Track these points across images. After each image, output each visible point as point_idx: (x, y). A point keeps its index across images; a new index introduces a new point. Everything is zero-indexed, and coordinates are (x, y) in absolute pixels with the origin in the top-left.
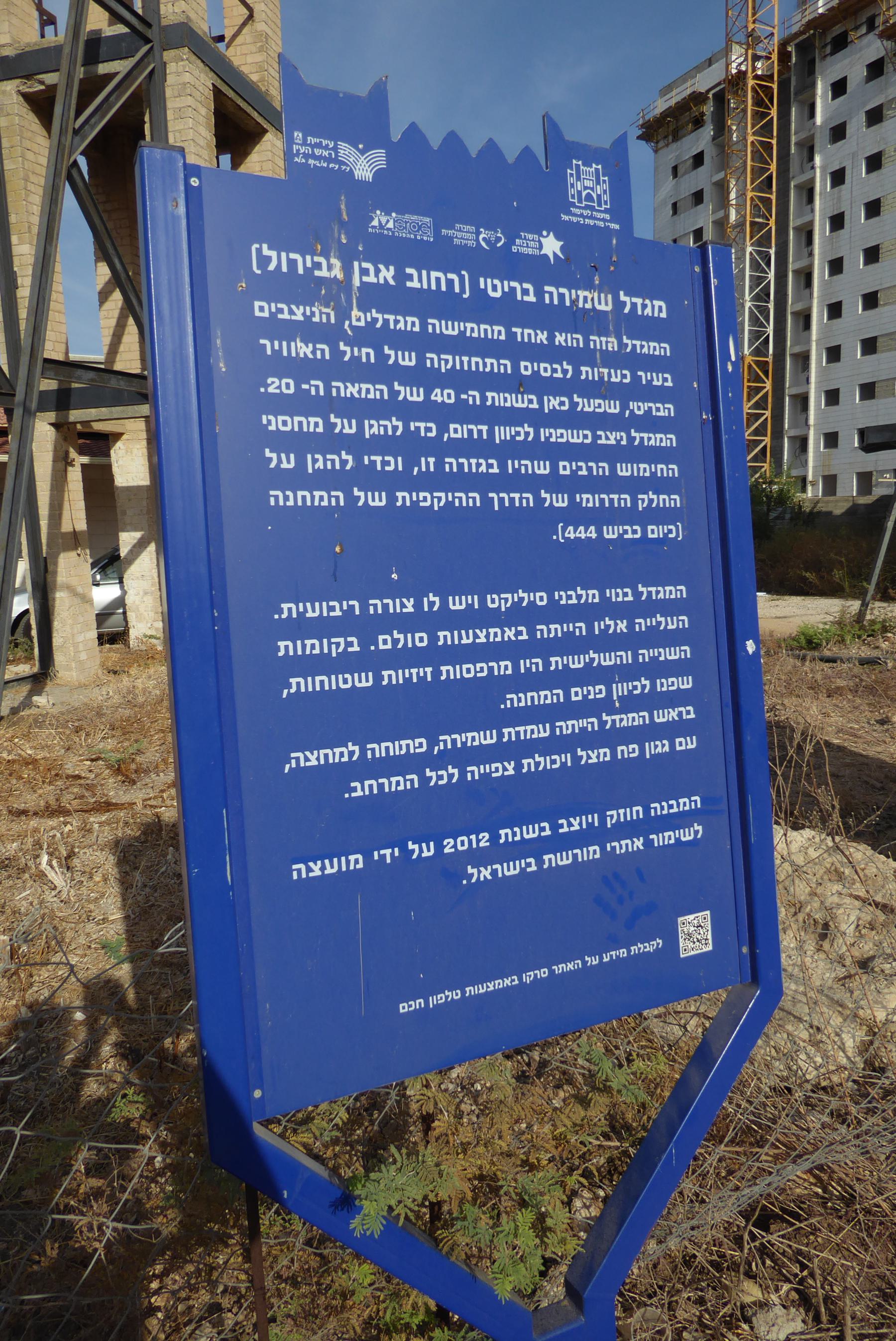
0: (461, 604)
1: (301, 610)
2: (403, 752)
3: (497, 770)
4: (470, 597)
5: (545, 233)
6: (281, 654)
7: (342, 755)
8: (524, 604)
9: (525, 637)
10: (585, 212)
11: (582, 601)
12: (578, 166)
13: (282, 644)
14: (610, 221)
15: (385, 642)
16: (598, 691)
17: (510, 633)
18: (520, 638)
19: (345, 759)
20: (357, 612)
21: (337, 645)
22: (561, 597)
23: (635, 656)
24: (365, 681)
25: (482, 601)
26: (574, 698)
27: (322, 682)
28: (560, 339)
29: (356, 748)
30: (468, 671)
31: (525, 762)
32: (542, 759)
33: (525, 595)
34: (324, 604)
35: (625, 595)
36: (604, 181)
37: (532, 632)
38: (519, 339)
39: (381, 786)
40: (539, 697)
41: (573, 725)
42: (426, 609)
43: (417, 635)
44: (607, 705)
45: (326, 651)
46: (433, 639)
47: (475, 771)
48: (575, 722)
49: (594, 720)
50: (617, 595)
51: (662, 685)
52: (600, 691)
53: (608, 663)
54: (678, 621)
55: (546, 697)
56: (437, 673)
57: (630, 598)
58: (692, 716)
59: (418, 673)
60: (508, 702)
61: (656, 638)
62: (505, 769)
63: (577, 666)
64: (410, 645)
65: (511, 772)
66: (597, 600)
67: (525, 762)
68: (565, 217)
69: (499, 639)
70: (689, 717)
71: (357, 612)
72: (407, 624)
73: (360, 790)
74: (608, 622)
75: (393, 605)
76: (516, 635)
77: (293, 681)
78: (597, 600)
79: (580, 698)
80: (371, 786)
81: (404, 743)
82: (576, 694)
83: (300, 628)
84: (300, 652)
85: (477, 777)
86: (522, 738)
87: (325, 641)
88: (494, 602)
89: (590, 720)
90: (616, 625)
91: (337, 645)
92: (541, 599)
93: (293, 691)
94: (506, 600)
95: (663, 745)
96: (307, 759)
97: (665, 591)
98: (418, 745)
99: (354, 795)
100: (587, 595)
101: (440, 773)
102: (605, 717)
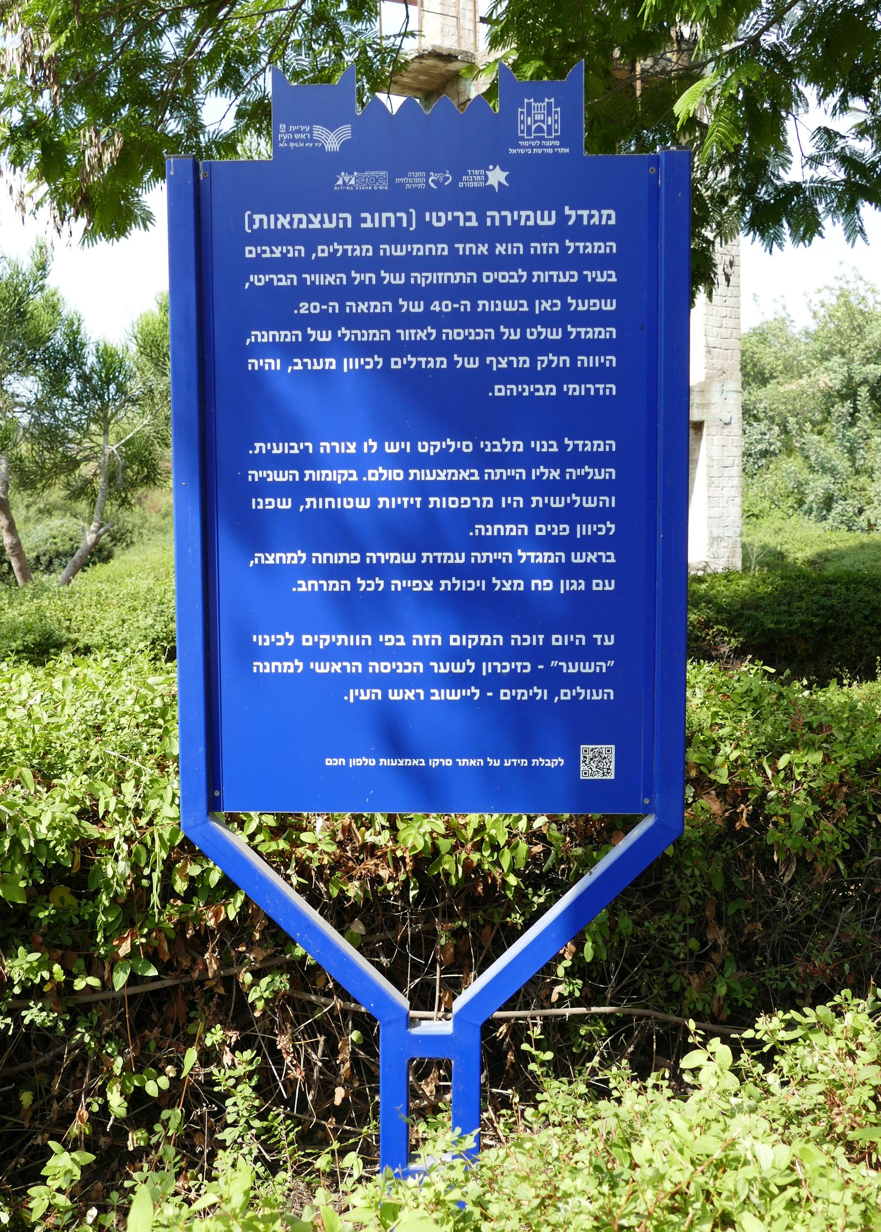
2: (341, 562)
5: (491, 167)
7: (292, 558)
10: (533, 144)
12: (529, 104)
14: (560, 147)
19: (295, 562)
28: (500, 249)
29: (304, 555)
31: (443, 582)
32: (458, 582)
36: (556, 112)
38: (461, 253)
48: (490, 554)
58: (613, 560)
62: (424, 586)
68: (513, 151)
80: (313, 585)
81: (342, 555)
95: (579, 584)
96: (266, 559)
99: (299, 589)
102: (520, 553)
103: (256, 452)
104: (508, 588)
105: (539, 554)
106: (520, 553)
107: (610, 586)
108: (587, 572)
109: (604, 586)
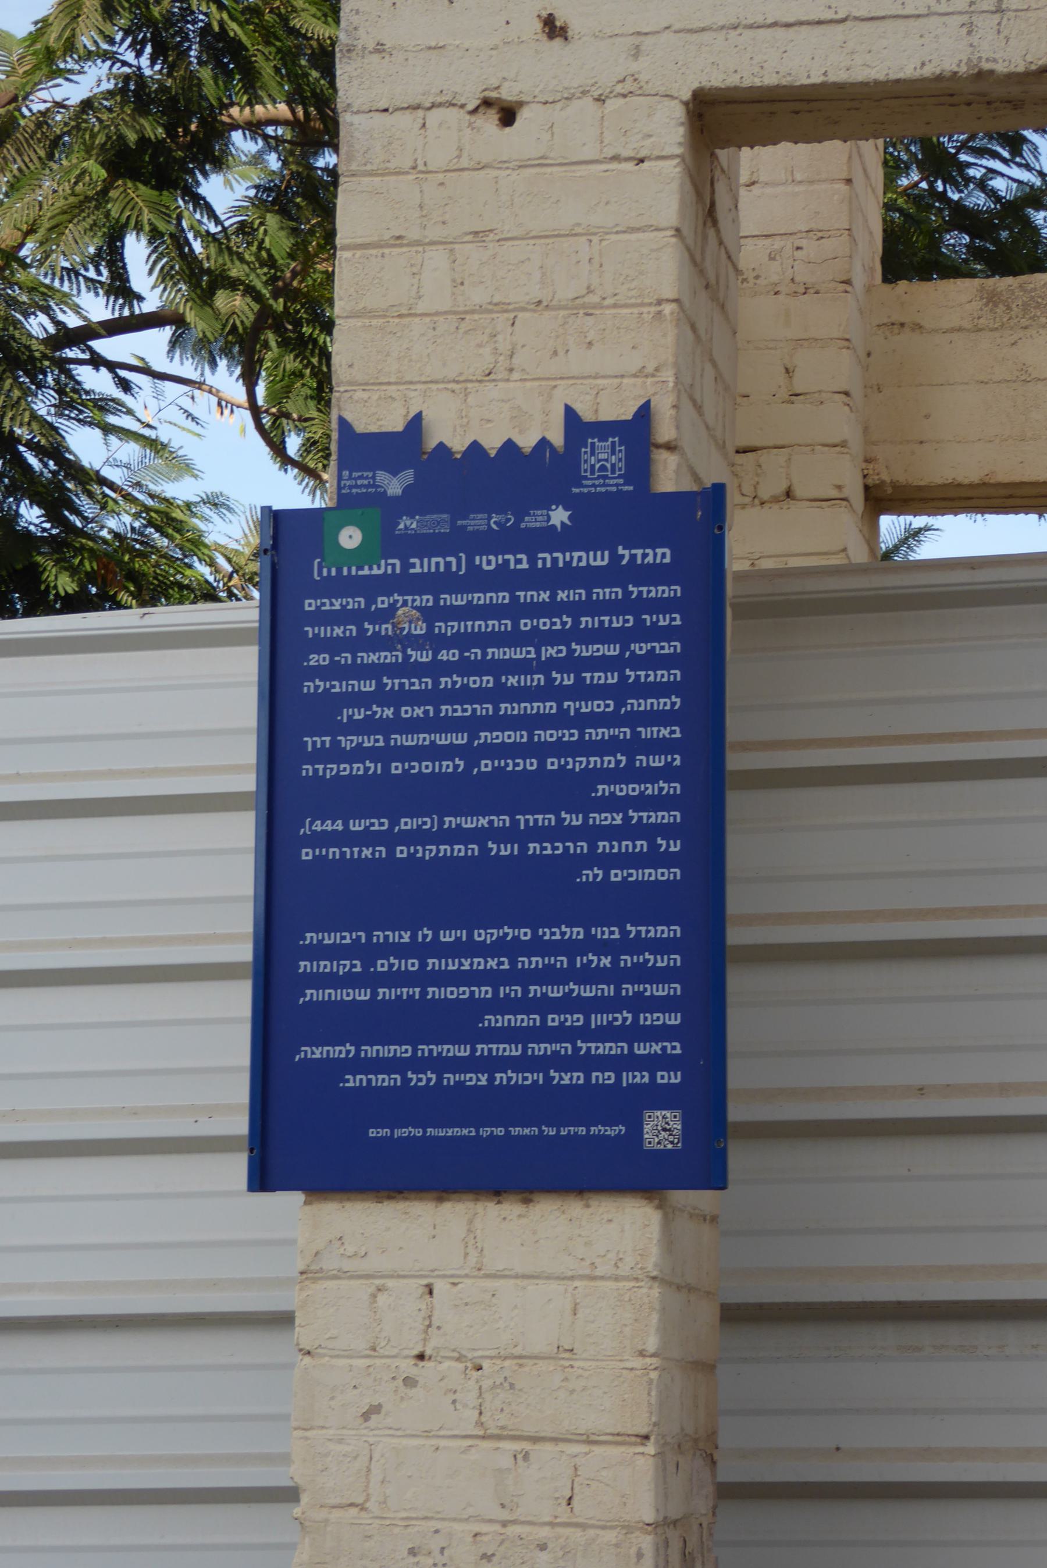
7: (340, 1052)
8: (509, 938)
9: (506, 966)
11: (566, 937)
15: (382, 965)
16: (576, 1020)
17: (492, 963)
18: (502, 967)
19: (343, 1056)
20: (363, 941)
21: (344, 966)
22: (544, 934)
23: (618, 990)
24: (364, 996)
25: (470, 935)
26: (550, 1024)
27: (330, 994)
29: (353, 1048)
31: (498, 1075)
35: (612, 933)
37: (513, 963)
39: (369, 1081)
40: (516, 1020)
42: (420, 940)
43: (410, 961)
44: (586, 1033)
45: (335, 970)
46: (423, 965)
49: (569, 1045)
50: (603, 933)
51: (646, 1019)
53: (588, 994)
54: (669, 959)
55: (522, 1020)
56: (424, 993)
57: (617, 936)
58: (678, 1051)
60: (486, 1022)
61: (643, 974)
62: (478, 1080)
63: (555, 995)
64: (403, 969)
65: (484, 1082)
66: (581, 937)
69: (481, 967)
70: (674, 1052)
71: (363, 941)
72: (402, 951)
73: (352, 1081)
74: (591, 957)
75: (393, 937)
77: (308, 992)
78: (581, 937)
80: (361, 1080)
81: (392, 1048)
84: (315, 970)
87: (335, 963)
88: (480, 936)
89: (563, 1045)
90: (599, 960)
91: (344, 966)
93: (307, 999)
94: (492, 935)
95: (643, 1077)
96: (313, 1053)
98: (404, 1051)
99: (347, 1085)
100: (572, 932)
103: (307, 942)
104: (566, 1082)
106: (579, 1044)
107: (676, 1079)
108: (652, 1063)
109: (669, 1078)
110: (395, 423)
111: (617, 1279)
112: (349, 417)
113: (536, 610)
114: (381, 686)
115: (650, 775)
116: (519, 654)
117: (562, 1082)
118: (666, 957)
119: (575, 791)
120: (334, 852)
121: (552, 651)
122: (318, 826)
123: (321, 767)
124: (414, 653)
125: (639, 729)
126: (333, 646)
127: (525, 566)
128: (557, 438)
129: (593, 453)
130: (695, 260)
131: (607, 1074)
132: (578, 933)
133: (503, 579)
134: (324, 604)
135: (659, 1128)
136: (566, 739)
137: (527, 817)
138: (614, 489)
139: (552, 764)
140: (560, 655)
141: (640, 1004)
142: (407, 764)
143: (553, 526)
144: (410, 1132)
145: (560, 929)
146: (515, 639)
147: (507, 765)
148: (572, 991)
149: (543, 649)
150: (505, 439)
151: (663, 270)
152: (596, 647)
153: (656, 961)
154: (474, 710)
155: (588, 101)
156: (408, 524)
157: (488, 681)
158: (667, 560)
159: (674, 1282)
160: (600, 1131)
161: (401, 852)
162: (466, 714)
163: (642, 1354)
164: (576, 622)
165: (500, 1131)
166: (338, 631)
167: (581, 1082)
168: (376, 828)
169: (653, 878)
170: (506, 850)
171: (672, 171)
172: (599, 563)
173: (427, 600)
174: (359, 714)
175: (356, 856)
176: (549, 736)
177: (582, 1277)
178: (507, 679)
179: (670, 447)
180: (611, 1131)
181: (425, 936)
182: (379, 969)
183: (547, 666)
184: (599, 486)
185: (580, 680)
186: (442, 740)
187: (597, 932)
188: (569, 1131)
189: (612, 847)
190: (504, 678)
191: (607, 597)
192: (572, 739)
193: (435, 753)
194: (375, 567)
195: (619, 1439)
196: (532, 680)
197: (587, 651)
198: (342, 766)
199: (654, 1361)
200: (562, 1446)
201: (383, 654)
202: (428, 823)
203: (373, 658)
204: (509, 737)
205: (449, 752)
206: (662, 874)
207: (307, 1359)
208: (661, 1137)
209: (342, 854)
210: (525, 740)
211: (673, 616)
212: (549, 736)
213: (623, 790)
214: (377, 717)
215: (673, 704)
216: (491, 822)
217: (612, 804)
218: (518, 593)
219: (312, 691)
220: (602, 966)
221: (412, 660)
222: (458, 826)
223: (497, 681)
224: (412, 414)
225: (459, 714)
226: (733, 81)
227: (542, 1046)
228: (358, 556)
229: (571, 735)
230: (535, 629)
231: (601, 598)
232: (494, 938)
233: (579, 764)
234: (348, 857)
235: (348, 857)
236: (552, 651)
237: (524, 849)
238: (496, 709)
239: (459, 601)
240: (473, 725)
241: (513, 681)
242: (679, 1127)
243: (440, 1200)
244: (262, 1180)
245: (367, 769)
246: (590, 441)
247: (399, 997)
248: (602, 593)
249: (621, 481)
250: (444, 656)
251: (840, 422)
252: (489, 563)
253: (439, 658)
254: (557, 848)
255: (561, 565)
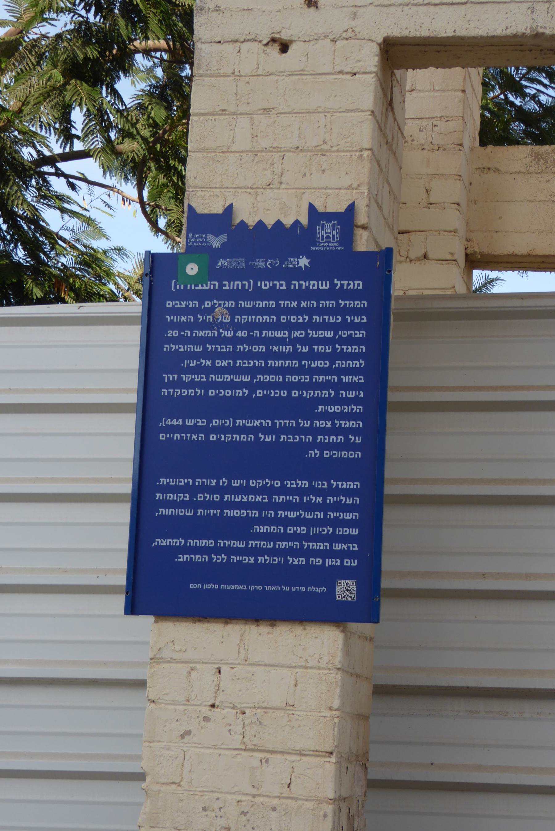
0: (237, 483)
1: (168, 481)
2: (203, 545)
3: (245, 559)
4: (242, 481)
6: (157, 498)
7: (176, 542)
8: (268, 485)
9: (266, 500)
11: (299, 486)
13: (158, 495)
15: (200, 497)
16: (303, 530)
17: (259, 498)
18: (264, 501)
19: (178, 544)
20: (191, 484)
22: (287, 484)
23: (325, 515)
24: (190, 513)
25: (248, 483)
27: (172, 512)
29: (183, 541)
30: (237, 513)
31: (260, 558)
32: (268, 558)
33: (269, 482)
34: (178, 480)
35: (324, 485)
37: (270, 499)
39: (191, 558)
41: (286, 545)
42: (221, 484)
43: (215, 496)
45: (175, 499)
46: (222, 498)
47: (234, 559)
50: (319, 484)
51: (339, 531)
52: (304, 530)
53: (309, 517)
55: (274, 529)
57: (326, 486)
58: (356, 549)
59: (213, 512)
63: (292, 516)
64: (211, 499)
65: (252, 561)
67: (260, 558)
69: (253, 500)
71: (191, 484)
74: (311, 497)
75: (207, 482)
76: (262, 499)
77: (160, 510)
79: (292, 532)
80: (187, 558)
81: (204, 541)
82: (290, 530)
83: (167, 489)
84: (164, 498)
85: (235, 561)
86: (258, 546)
87: (175, 495)
88: (253, 483)
89: (295, 543)
90: (316, 499)
92: (277, 484)
93: (160, 514)
94: (259, 483)
95: (337, 562)
96: (162, 542)
97: (347, 485)
98: (210, 543)
99: (179, 560)
100: (302, 484)
101: (218, 557)
102: (304, 543)
104: (296, 563)
105: (315, 544)
107: (354, 563)
108: (342, 555)
109: (351, 563)
110: (218, 209)
111: (319, 668)
112: (193, 205)
113: (289, 311)
114: (205, 348)
115: (347, 402)
116: (279, 335)
117: (294, 563)
118: (351, 499)
119: (307, 408)
120: (177, 436)
121: (297, 334)
122: (169, 422)
123: (172, 391)
124: (223, 332)
125: (342, 377)
126: (181, 326)
127: (284, 287)
128: (304, 221)
129: (323, 229)
130: (381, 128)
131: (317, 560)
132: (305, 484)
133: (272, 294)
134: (177, 304)
135: (344, 589)
136: (303, 381)
137: (280, 421)
138: (334, 248)
139: (295, 394)
140: (301, 336)
141: (337, 523)
142: (217, 391)
143: (301, 267)
144: (212, 586)
145: (296, 481)
146: (278, 326)
147: (271, 393)
148: (301, 515)
149: (293, 332)
150: (277, 220)
151: (364, 133)
152: (320, 332)
153: (346, 500)
154: (254, 364)
155: (327, 41)
156: (223, 263)
157: (262, 348)
158: (360, 287)
159: (349, 671)
160: (313, 590)
161: (213, 437)
162: (250, 365)
163: (330, 709)
164: (311, 319)
165: (260, 588)
166: (184, 319)
167: (304, 563)
168: (200, 424)
169: (346, 456)
170: (268, 438)
171: (371, 79)
172: (324, 287)
173: (232, 304)
174: (193, 363)
175: (189, 439)
176: (294, 378)
177: (300, 667)
178: (273, 348)
179: (364, 227)
180: (319, 590)
181: (224, 483)
182: (199, 499)
183: (294, 342)
184: (326, 246)
185: (311, 350)
186: (237, 379)
187: (315, 484)
188: (297, 589)
189: (325, 439)
190: (271, 347)
191: (328, 306)
192: (306, 381)
193: (233, 385)
194: (204, 285)
195: (317, 753)
196: (286, 349)
197: (316, 334)
198: (183, 391)
199: (337, 713)
200: (286, 756)
201: (207, 332)
202: (228, 423)
203: (202, 333)
204: (273, 378)
205: (241, 385)
206: (351, 455)
207: (152, 705)
208: (345, 594)
209: (182, 437)
210: (281, 380)
211: (362, 317)
212: (294, 378)
213: (332, 409)
214: (203, 365)
215: (361, 364)
216: (261, 423)
217: (326, 416)
218: (280, 302)
219: (168, 350)
220: (317, 502)
221: (222, 336)
222: (244, 425)
223: (267, 348)
224: (227, 205)
225: (246, 365)
226: (405, 33)
227: (284, 543)
228: (196, 279)
229: (305, 379)
230: (289, 321)
231: (324, 306)
232: (260, 485)
233: (309, 394)
234: (184, 439)
235: (184, 439)
236: (297, 334)
237: (278, 438)
238: (266, 363)
239: (249, 305)
240: (253, 371)
241: (275, 349)
242: (355, 589)
243: (226, 623)
244: (132, 609)
245: (196, 393)
246: (321, 222)
247: (209, 515)
248: (324, 304)
249: (338, 244)
250: (239, 334)
251: (454, 219)
252: (265, 285)
253: (237, 335)
254: (296, 439)
255: (304, 288)
